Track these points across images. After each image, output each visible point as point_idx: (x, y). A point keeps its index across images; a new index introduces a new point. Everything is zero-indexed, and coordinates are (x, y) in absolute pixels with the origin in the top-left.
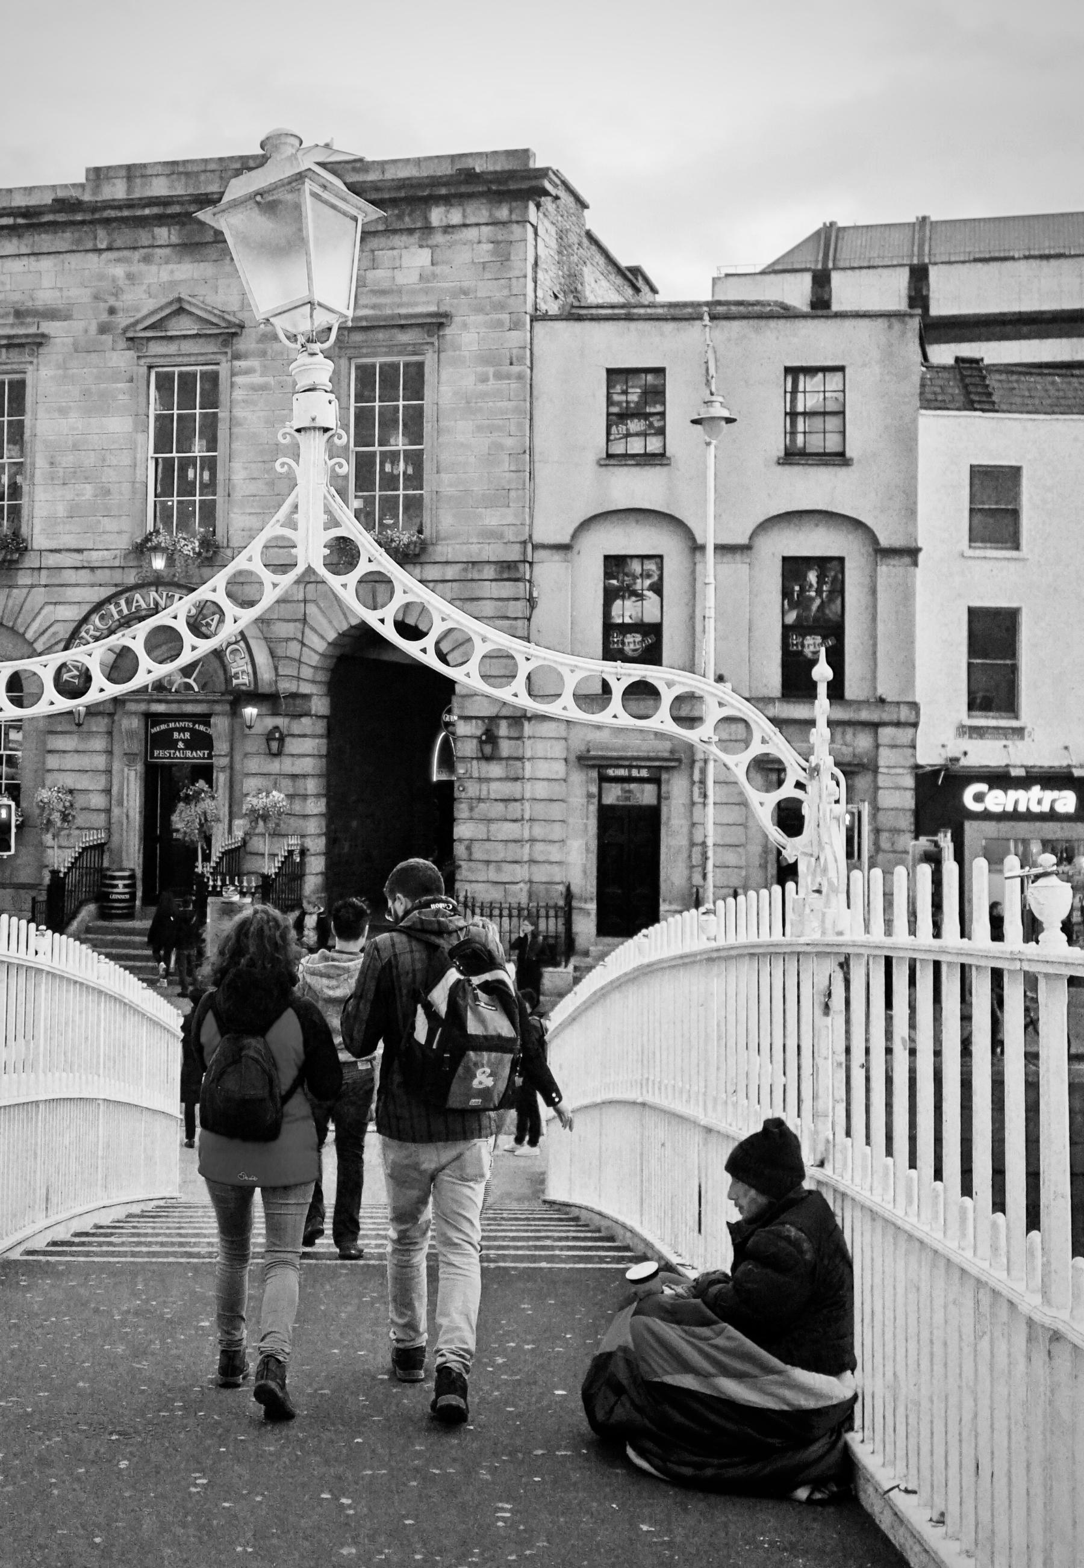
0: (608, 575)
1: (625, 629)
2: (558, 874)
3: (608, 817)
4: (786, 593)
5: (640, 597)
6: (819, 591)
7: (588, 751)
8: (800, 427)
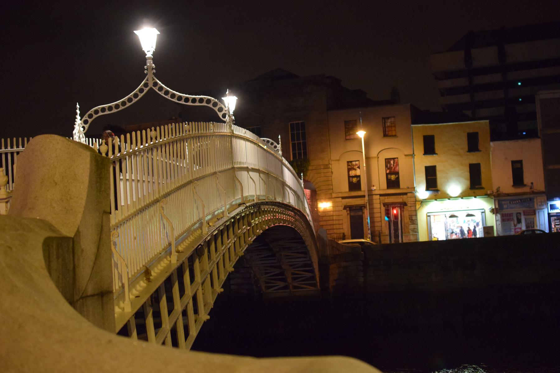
0: (348, 165)
1: (353, 177)
2: (342, 231)
3: (352, 218)
4: (386, 166)
5: (355, 170)
6: (394, 165)
7: (347, 204)
8: (387, 130)
